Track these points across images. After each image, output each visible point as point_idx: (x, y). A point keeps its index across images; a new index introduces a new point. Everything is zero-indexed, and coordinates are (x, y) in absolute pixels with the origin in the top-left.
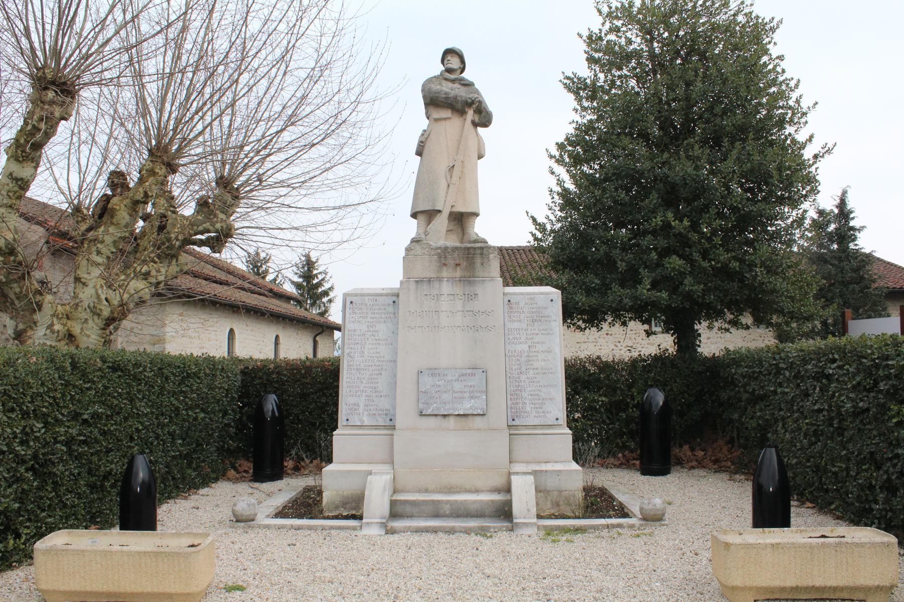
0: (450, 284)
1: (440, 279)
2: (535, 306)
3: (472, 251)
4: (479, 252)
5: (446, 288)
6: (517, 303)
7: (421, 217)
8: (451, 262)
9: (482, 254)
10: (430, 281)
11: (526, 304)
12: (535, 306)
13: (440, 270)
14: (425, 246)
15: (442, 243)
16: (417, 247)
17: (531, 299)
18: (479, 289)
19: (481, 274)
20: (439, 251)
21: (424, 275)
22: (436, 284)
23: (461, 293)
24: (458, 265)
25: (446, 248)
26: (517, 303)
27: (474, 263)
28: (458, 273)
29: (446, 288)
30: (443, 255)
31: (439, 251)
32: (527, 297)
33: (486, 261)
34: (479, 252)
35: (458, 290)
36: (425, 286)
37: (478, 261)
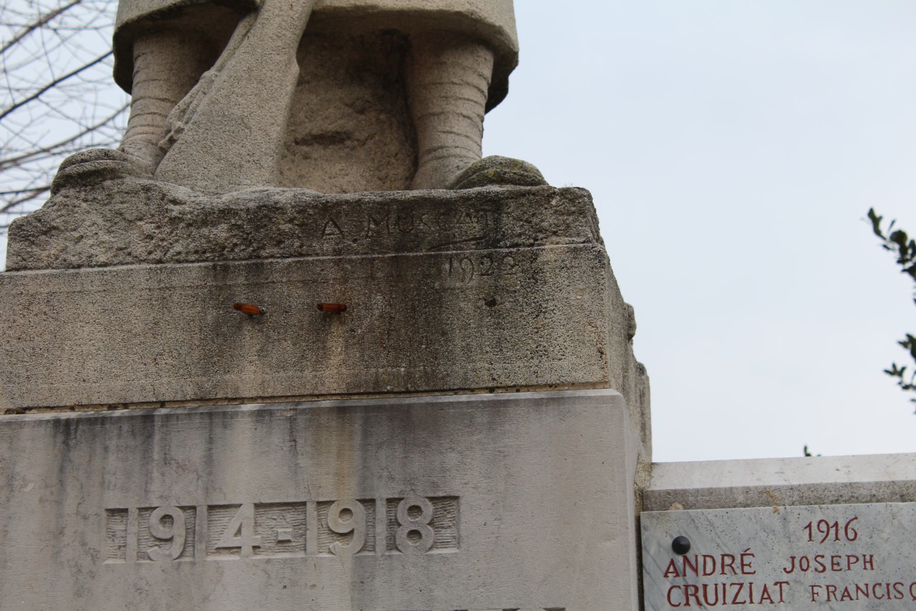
0: (278, 437)
1: (213, 409)
2: (859, 576)
3: (426, 225)
4: (474, 227)
5: (250, 463)
6: (739, 562)
7: (150, 63)
8: (290, 296)
9: (490, 240)
10: (145, 420)
11: (799, 563)
12: (859, 576)
13: (217, 347)
14: (134, 206)
15: (253, 187)
16: (89, 216)
17: (831, 528)
18: (465, 467)
19: (482, 367)
20: (221, 232)
21: (104, 391)
22: (189, 443)
23: (348, 496)
24: (333, 313)
25: (265, 213)
26: (739, 562)
27: (438, 298)
28: (336, 368)
29: (250, 463)
30: (240, 266)
31: (221, 232)
32: (804, 514)
33: (515, 279)
34: (474, 227)
35: (329, 472)
36: (113, 468)
37: (466, 281)
